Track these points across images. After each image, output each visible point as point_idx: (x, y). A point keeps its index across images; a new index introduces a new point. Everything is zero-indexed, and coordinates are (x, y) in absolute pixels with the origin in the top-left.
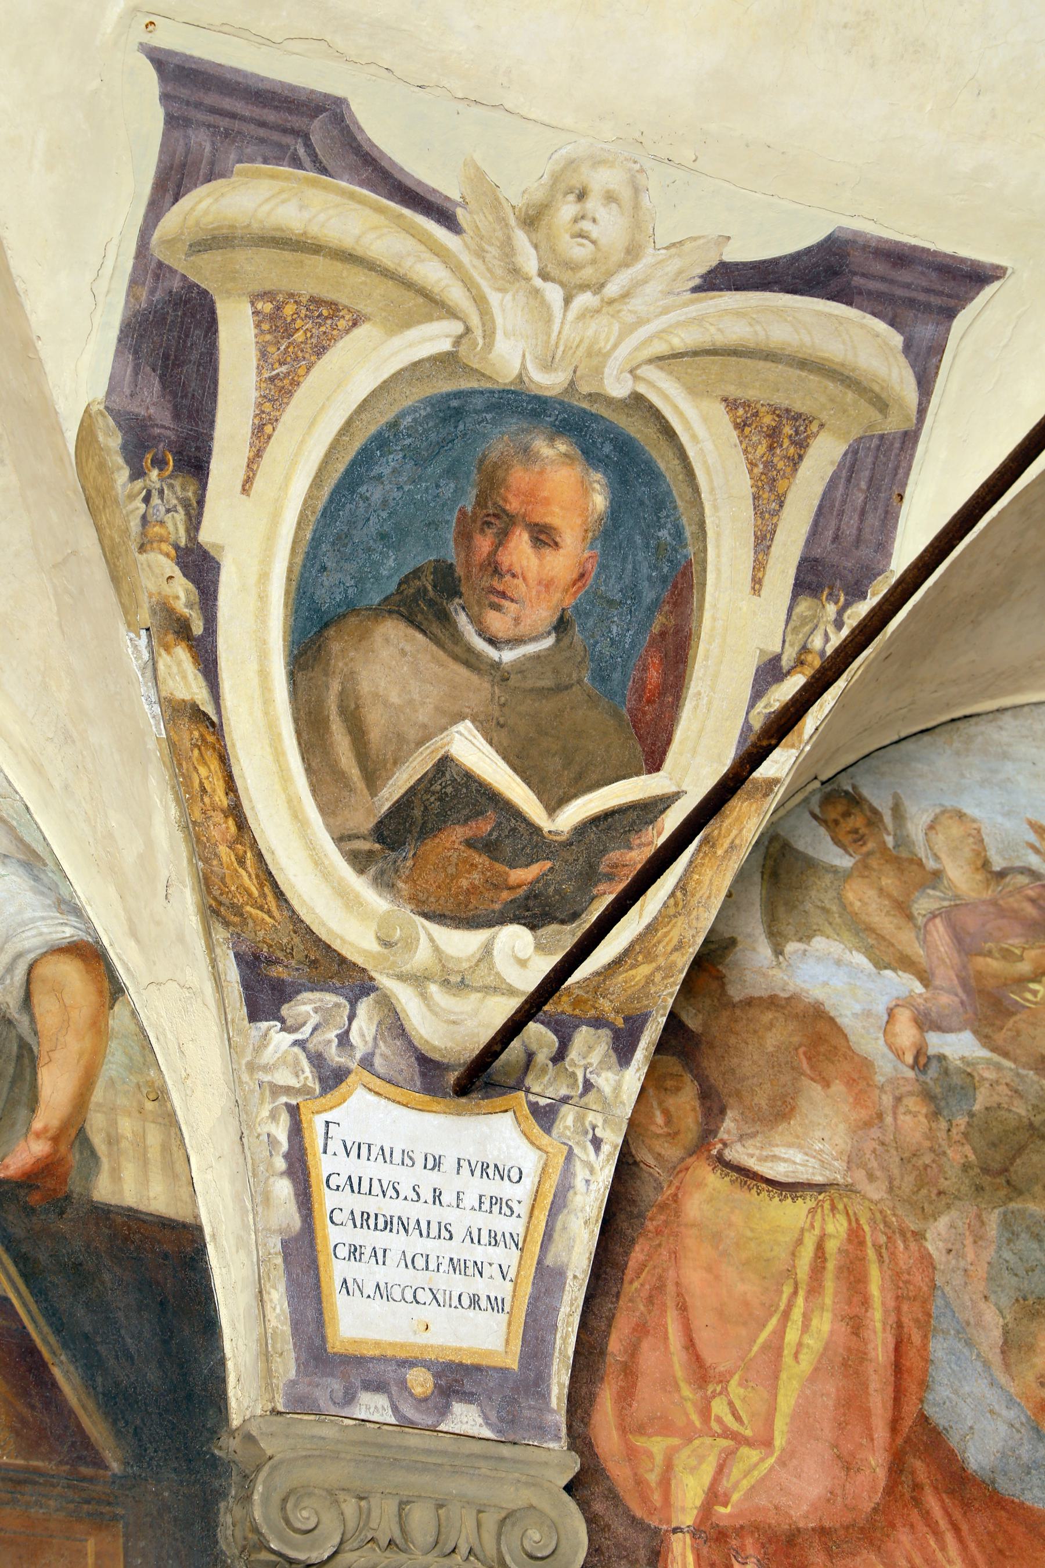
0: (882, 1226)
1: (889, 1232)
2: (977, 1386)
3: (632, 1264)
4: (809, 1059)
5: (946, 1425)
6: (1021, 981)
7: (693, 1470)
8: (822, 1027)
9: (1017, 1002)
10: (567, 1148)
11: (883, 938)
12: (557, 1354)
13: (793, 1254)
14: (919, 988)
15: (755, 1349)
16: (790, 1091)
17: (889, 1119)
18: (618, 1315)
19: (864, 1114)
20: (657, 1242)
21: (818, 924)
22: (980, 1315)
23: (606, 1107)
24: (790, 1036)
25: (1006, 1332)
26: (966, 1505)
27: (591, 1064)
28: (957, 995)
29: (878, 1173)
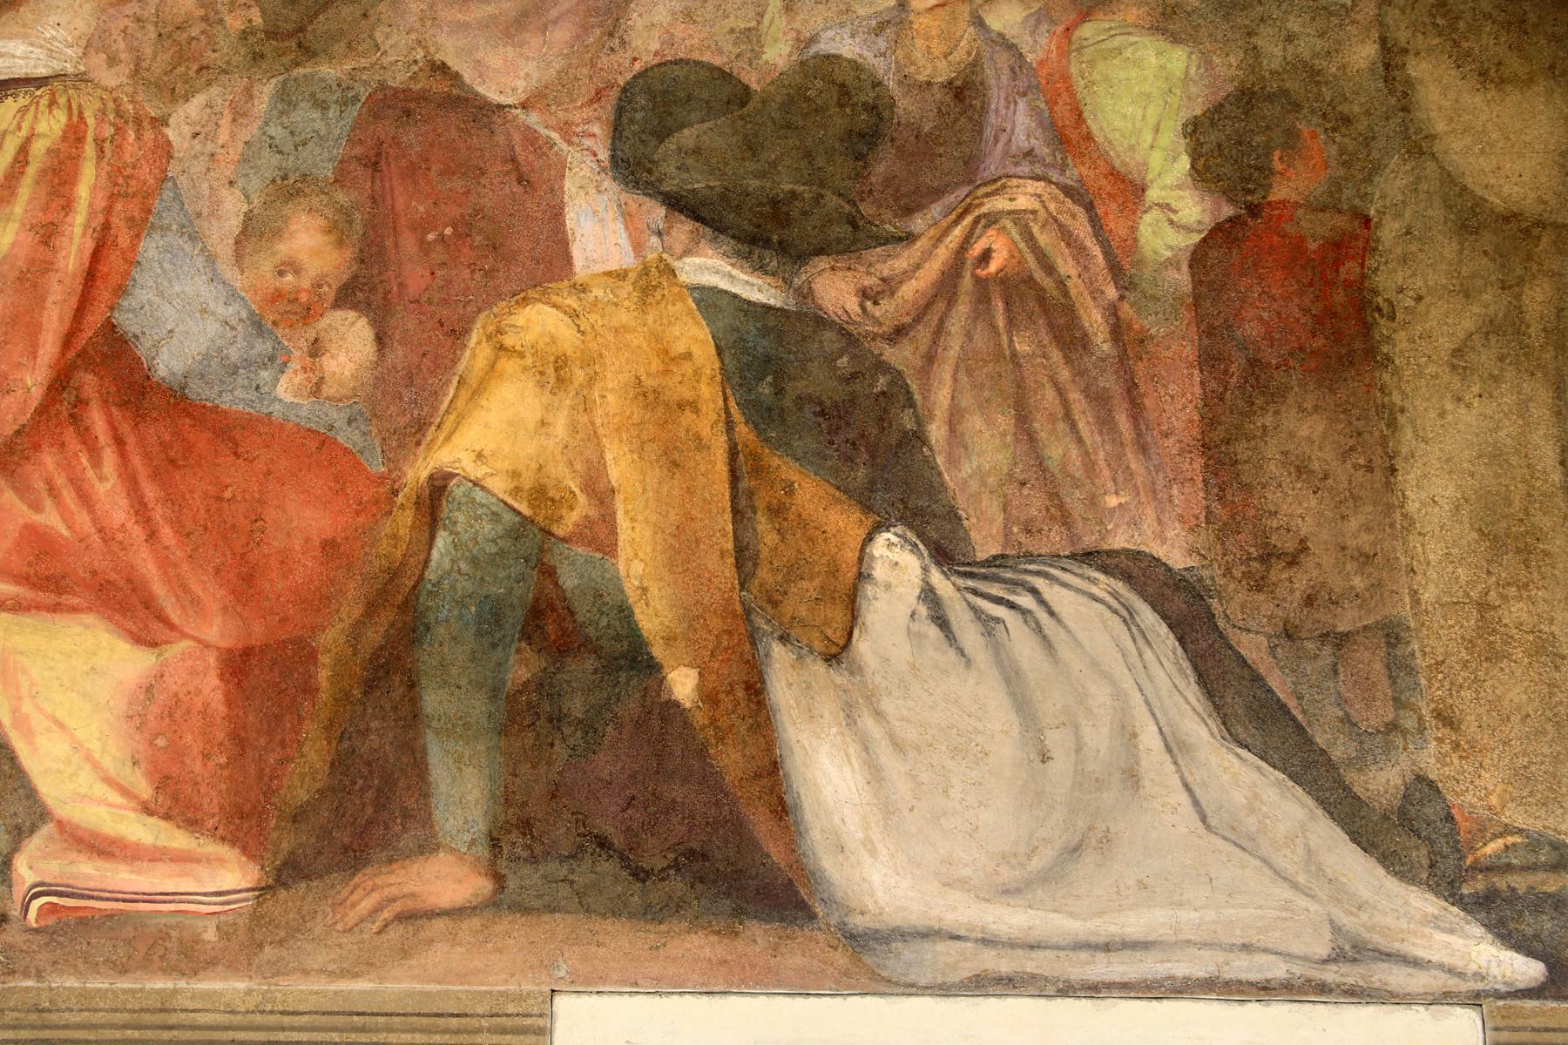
0: (111, 117)
1: (120, 122)
2: (195, 286)
5: (138, 332)
22: (216, 204)
25: (248, 218)
26: (139, 417)
29: (123, 56)
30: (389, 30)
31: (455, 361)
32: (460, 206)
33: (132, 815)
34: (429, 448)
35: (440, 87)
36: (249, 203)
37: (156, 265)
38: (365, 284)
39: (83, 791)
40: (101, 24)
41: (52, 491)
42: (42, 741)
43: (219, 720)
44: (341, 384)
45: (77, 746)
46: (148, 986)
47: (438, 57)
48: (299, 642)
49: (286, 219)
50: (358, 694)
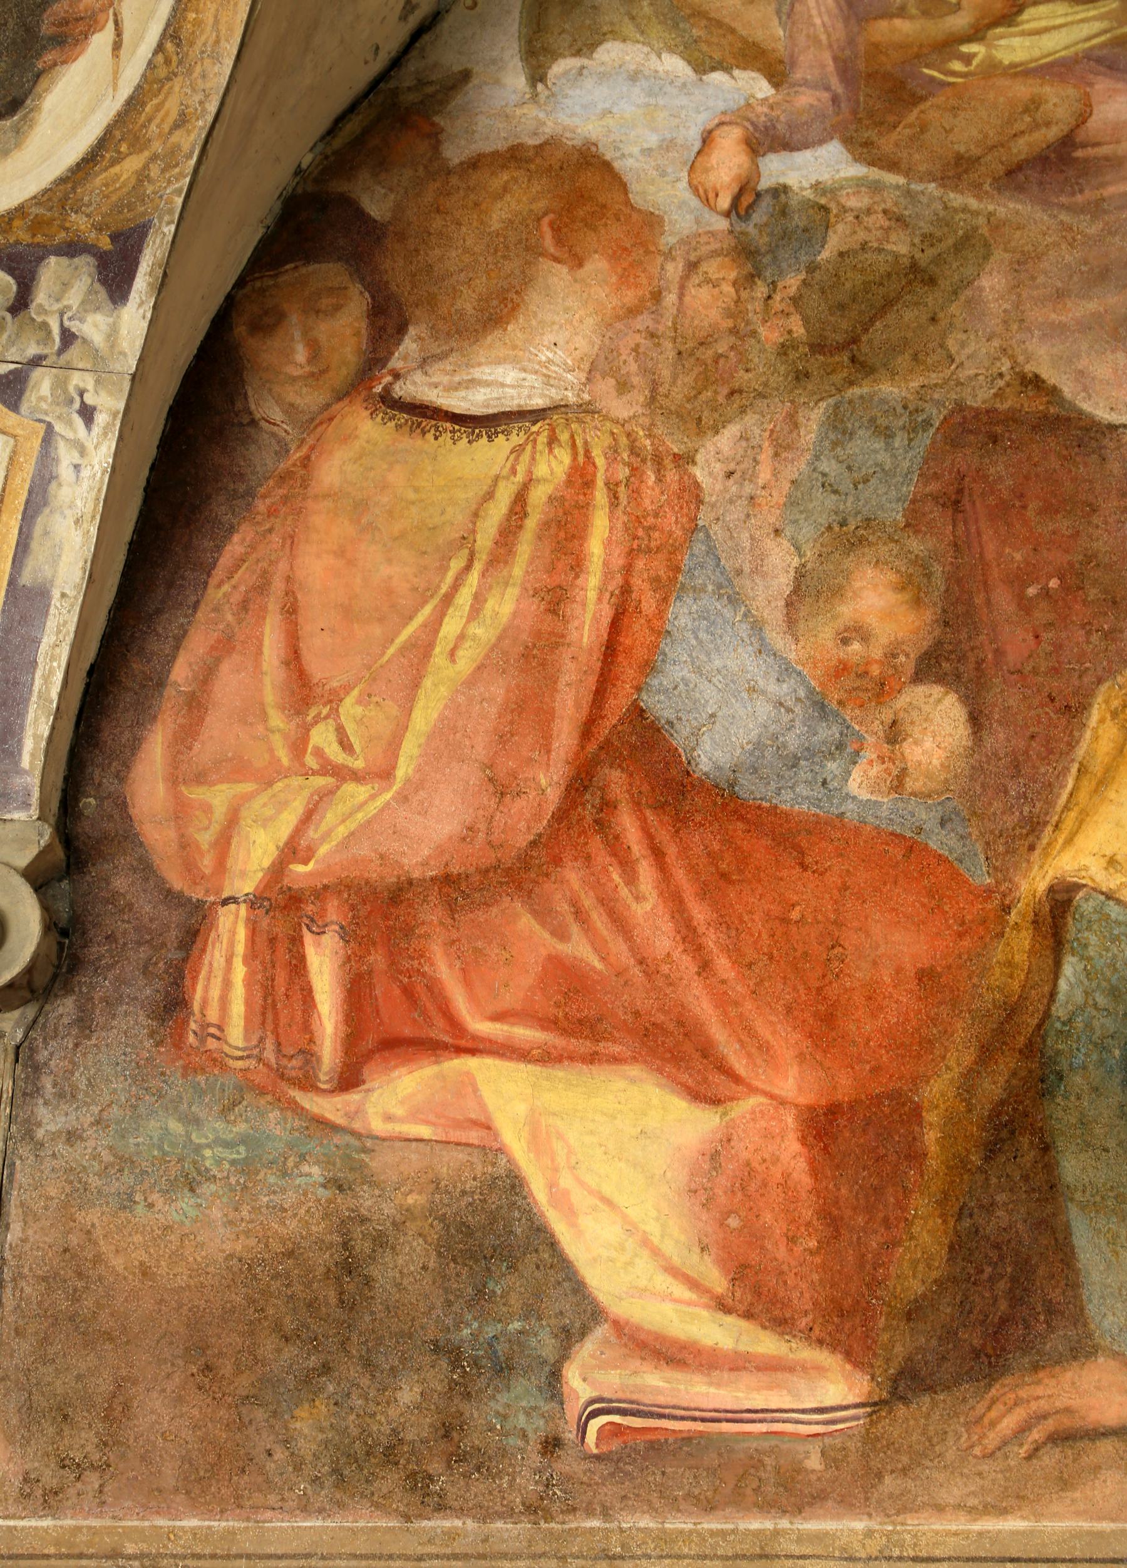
0: (625, 455)
3: (225, 560)
4: (556, 230)
5: (672, 717)
6: (948, 45)
7: (265, 822)
8: (589, 179)
9: (932, 79)
10: (44, 426)
11: (719, 24)
12: (34, 699)
13: (476, 515)
14: (762, 88)
15: (391, 651)
16: (515, 282)
17: (671, 299)
18: (192, 631)
19: (630, 296)
20: (268, 526)
21: (612, 24)
22: (762, 557)
23: (98, 364)
24: (534, 200)
25: (801, 574)
26: (680, 822)
27: (69, 308)
28: (827, 88)
29: (635, 380)
30: (964, 337)
31: (1072, 745)
32: (1067, 551)
33: (705, 1313)
34: (1046, 853)
35: (1033, 405)
36: (800, 556)
37: (689, 635)
38: (951, 652)
39: (643, 1283)
40: (607, 341)
41: (579, 914)
42: (586, 1222)
43: (804, 1195)
44: (929, 776)
45: (630, 1228)
46: (742, 1526)
47: (1029, 368)
48: (896, 1096)
49: (848, 575)
50: (976, 1159)
